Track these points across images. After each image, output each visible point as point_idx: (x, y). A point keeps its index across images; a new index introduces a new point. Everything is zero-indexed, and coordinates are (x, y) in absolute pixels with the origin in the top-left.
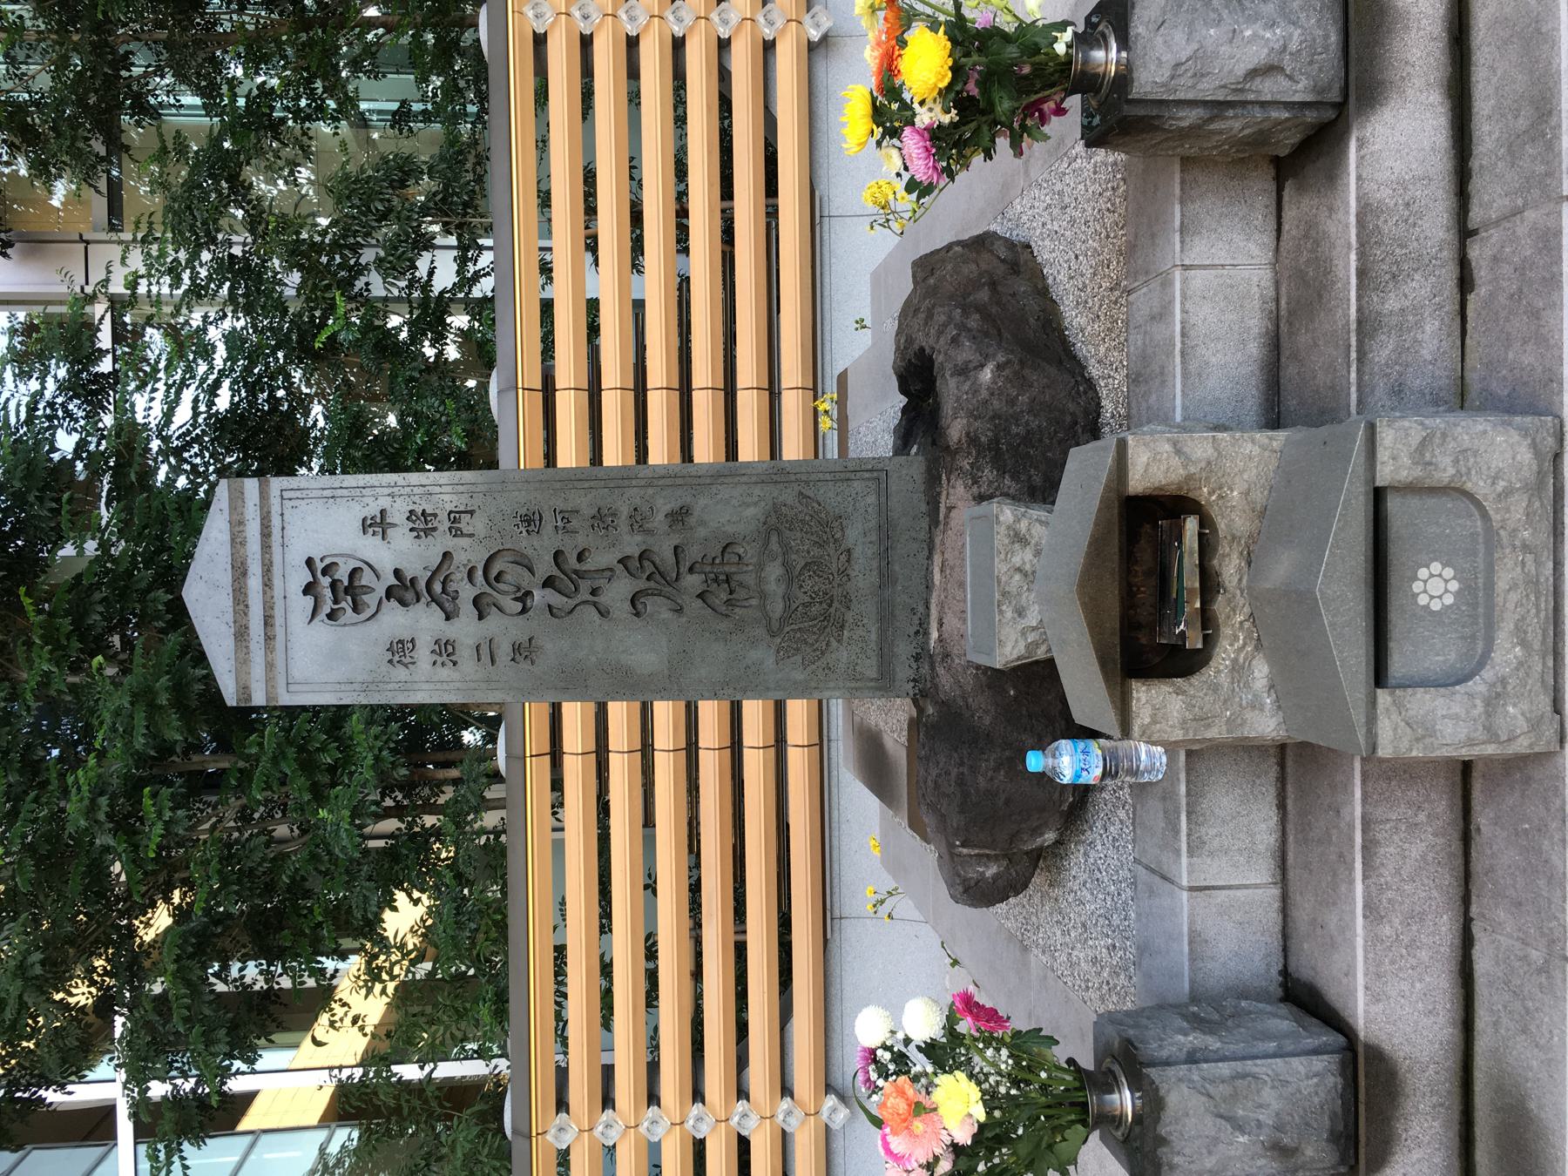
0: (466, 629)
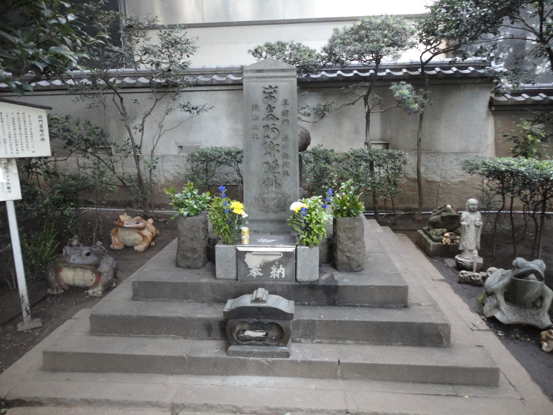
0: (261, 123)
